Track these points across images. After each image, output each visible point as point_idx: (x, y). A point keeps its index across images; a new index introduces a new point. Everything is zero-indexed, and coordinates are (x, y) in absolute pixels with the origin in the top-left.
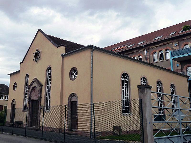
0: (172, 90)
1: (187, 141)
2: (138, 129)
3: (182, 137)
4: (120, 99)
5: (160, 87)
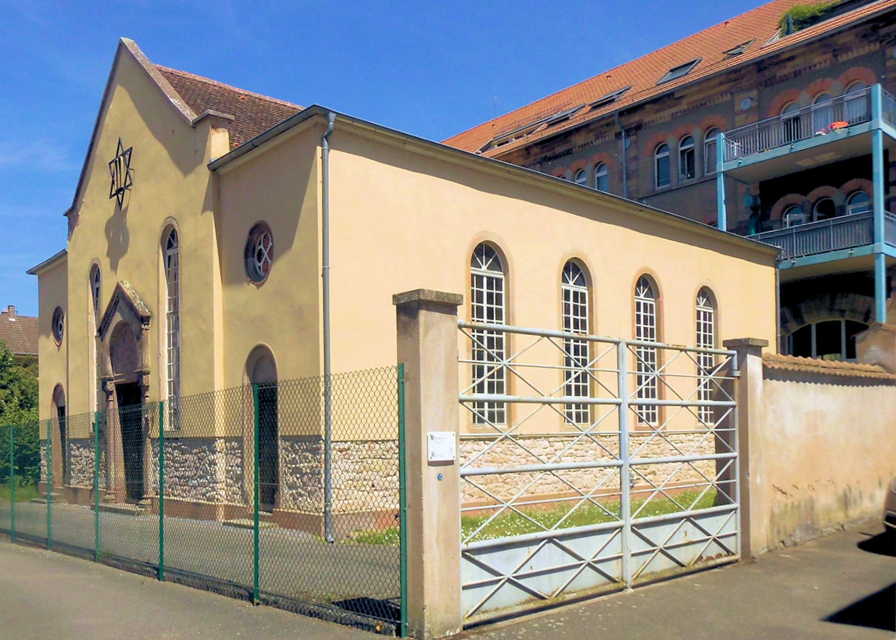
0: (576, 293)
1: (655, 546)
2: (393, 507)
3: (627, 530)
4: (392, 361)
5: (582, 289)
